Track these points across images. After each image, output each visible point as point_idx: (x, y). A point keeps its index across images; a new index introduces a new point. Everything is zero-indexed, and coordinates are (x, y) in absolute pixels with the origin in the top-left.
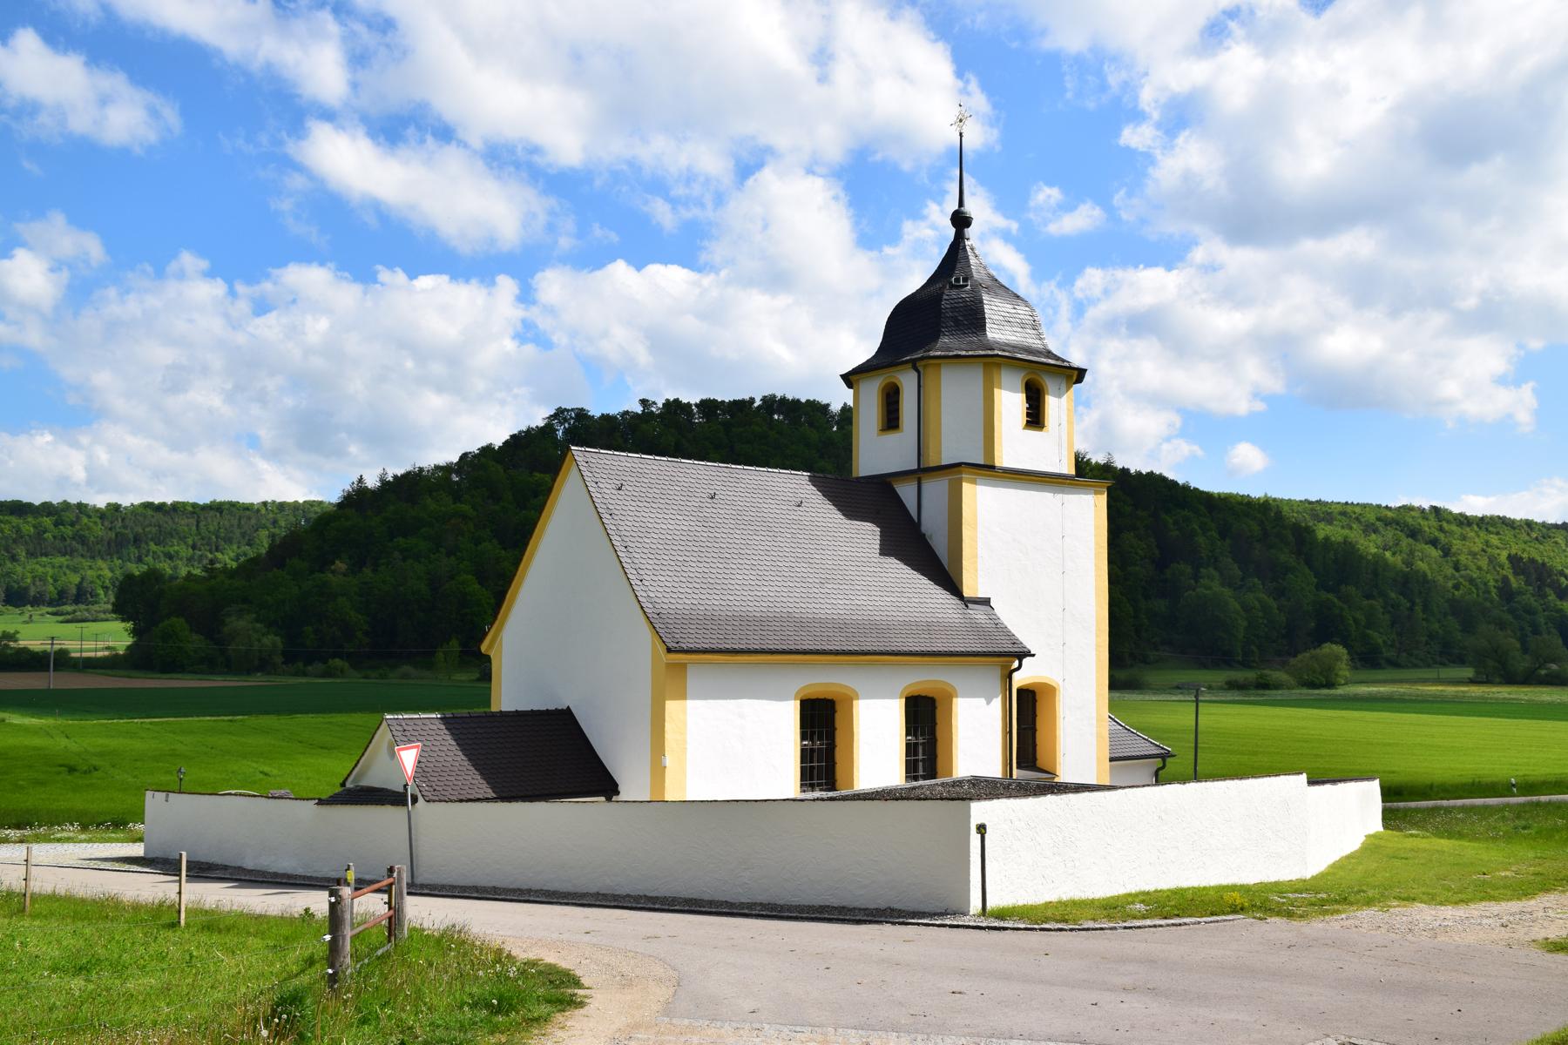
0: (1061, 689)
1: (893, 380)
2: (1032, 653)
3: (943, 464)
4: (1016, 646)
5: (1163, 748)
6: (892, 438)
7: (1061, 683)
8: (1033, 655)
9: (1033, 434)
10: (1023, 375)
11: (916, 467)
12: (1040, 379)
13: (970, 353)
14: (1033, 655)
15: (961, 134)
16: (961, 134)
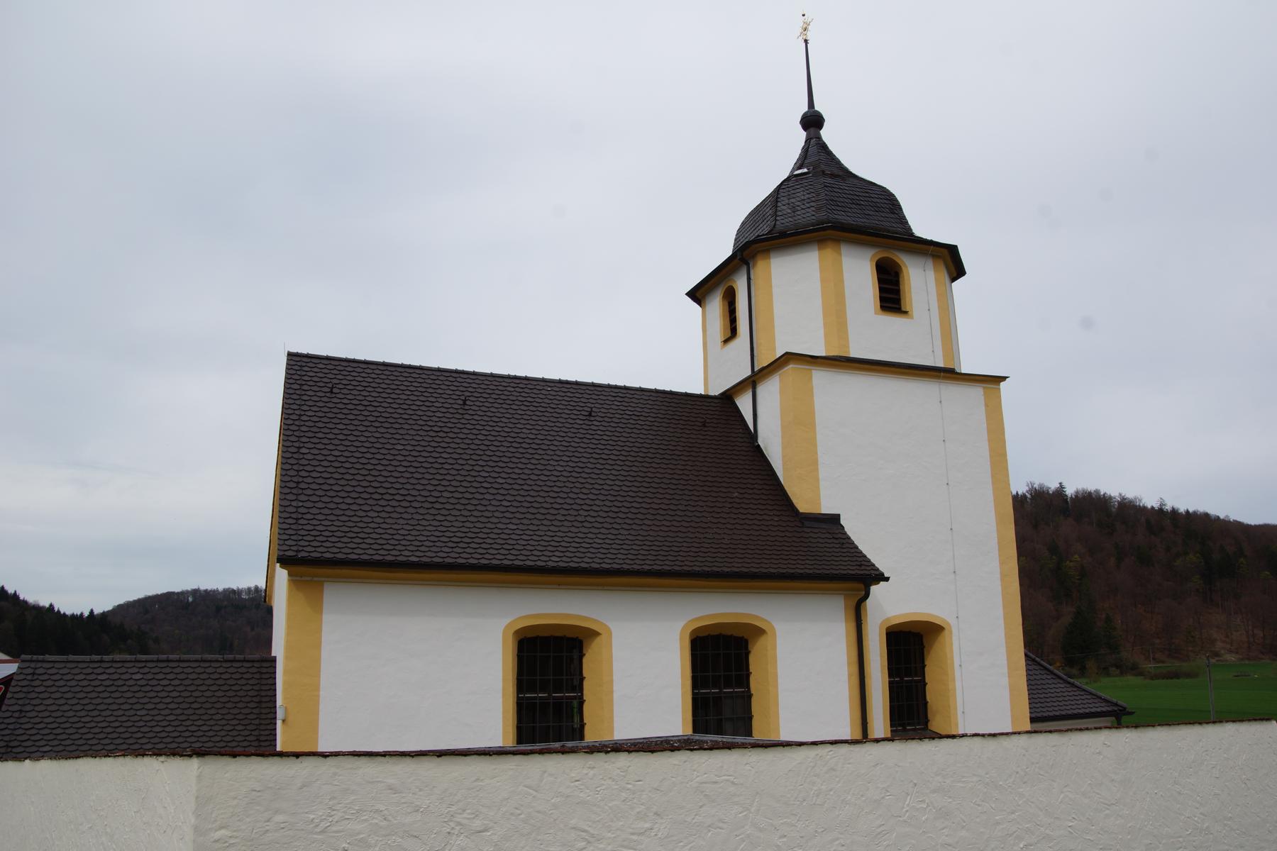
0: (954, 631)
2: (886, 575)
4: (863, 567)
5: (1116, 705)
6: (734, 344)
8: (887, 579)
12: (897, 260)
14: (887, 579)
15: (806, 41)
16: (806, 41)
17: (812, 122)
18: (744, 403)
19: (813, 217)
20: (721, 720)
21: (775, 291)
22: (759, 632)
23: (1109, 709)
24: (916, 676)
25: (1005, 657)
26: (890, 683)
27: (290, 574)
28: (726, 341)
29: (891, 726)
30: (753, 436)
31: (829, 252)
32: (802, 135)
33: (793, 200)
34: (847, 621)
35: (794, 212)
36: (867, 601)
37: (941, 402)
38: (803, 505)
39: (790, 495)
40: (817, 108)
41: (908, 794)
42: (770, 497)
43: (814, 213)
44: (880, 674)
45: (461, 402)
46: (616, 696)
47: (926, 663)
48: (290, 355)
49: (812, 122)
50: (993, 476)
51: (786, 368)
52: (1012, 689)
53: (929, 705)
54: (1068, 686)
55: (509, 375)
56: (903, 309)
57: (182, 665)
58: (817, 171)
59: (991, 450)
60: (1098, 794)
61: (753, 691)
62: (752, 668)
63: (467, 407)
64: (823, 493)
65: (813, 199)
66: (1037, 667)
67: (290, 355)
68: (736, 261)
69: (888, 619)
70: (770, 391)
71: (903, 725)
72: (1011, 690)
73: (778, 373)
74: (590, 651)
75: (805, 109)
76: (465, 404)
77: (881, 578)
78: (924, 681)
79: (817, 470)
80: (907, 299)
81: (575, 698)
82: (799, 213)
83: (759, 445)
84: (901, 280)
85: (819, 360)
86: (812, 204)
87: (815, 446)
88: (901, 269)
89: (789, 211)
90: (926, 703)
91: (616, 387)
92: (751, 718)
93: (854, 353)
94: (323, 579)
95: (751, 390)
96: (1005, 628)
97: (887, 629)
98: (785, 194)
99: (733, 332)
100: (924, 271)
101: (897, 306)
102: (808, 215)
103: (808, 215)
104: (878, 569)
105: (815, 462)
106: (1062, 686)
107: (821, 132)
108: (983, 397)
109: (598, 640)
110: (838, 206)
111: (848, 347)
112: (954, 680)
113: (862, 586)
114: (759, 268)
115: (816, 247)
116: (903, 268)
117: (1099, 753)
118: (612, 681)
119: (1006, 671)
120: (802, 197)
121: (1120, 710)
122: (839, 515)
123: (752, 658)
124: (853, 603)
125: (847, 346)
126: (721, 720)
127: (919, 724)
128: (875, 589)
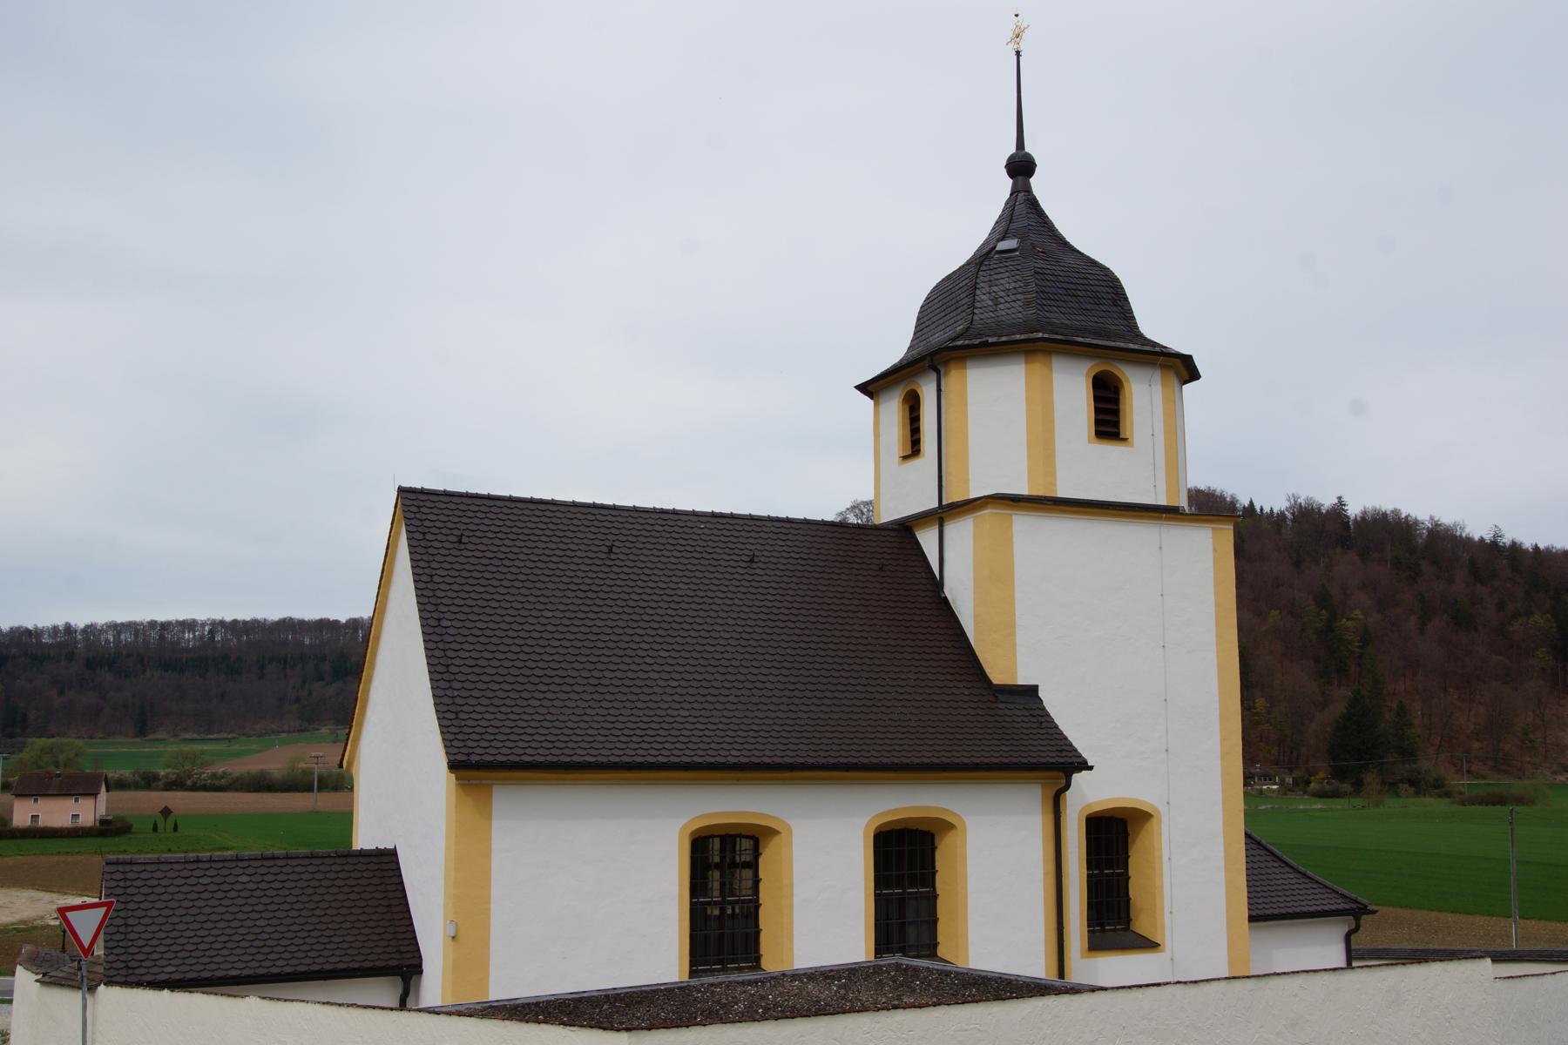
0: (1164, 819)
1: (915, 388)
3: (972, 496)
4: (1064, 754)
5: (1355, 901)
6: (915, 463)
7: (1161, 807)
8: (1091, 768)
9: (1109, 449)
10: (1085, 372)
11: (936, 505)
12: (1116, 373)
13: (1004, 339)
14: (1091, 768)
15: (1018, 53)
17: (1021, 167)
18: (927, 539)
19: (1020, 315)
20: (904, 924)
21: (971, 410)
22: (948, 826)
23: (1346, 906)
25: (1222, 848)
26: (1089, 876)
27: (456, 779)
28: (905, 458)
29: (1089, 926)
30: (938, 585)
31: (1038, 367)
32: (1007, 183)
33: (995, 289)
35: (996, 305)
37: (1160, 548)
38: (997, 677)
40: (1028, 149)
41: (1117, 1036)
42: (961, 664)
43: (1020, 309)
45: (606, 550)
46: (796, 900)
48: (401, 490)
49: (1021, 167)
51: (979, 514)
52: (1229, 885)
53: (1131, 902)
55: (654, 508)
56: (1121, 436)
57: (294, 862)
58: (1027, 250)
60: (1293, 1034)
61: (939, 891)
63: (613, 556)
64: (1020, 659)
65: (1020, 290)
66: (1262, 852)
67: (401, 490)
68: (926, 363)
69: (1089, 805)
70: (961, 533)
71: (1102, 925)
72: (1227, 887)
74: (767, 850)
75: (1013, 150)
76: (610, 552)
77: (1084, 766)
78: (1127, 874)
79: (1013, 634)
80: (1128, 423)
81: (750, 901)
82: (1001, 306)
83: (946, 597)
84: (1121, 397)
86: (1019, 296)
88: (1122, 384)
89: (990, 303)
90: (1128, 900)
91: (778, 520)
92: (935, 921)
93: (1062, 493)
94: (490, 782)
95: (937, 526)
98: (986, 279)
99: (914, 448)
100: (1150, 386)
101: (1114, 430)
102: (1013, 310)
103: (1013, 310)
105: (1013, 625)
107: (1032, 180)
108: (1211, 540)
109: (776, 840)
110: (1050, 299)
111: (1055, 485)
112: (1162, 875)
113: (1062, 774)
114: (952, 379)
115: (1023, 359)
116: (1125, 384)
117: (1295, 996)
118: (791, 885)
119: (1222, 864)
120: (1007, 286)
121: (1359, 909)
125: (1054, 484)
126: (904, 924)
127: (1119, 924)
128: (1078, 778)
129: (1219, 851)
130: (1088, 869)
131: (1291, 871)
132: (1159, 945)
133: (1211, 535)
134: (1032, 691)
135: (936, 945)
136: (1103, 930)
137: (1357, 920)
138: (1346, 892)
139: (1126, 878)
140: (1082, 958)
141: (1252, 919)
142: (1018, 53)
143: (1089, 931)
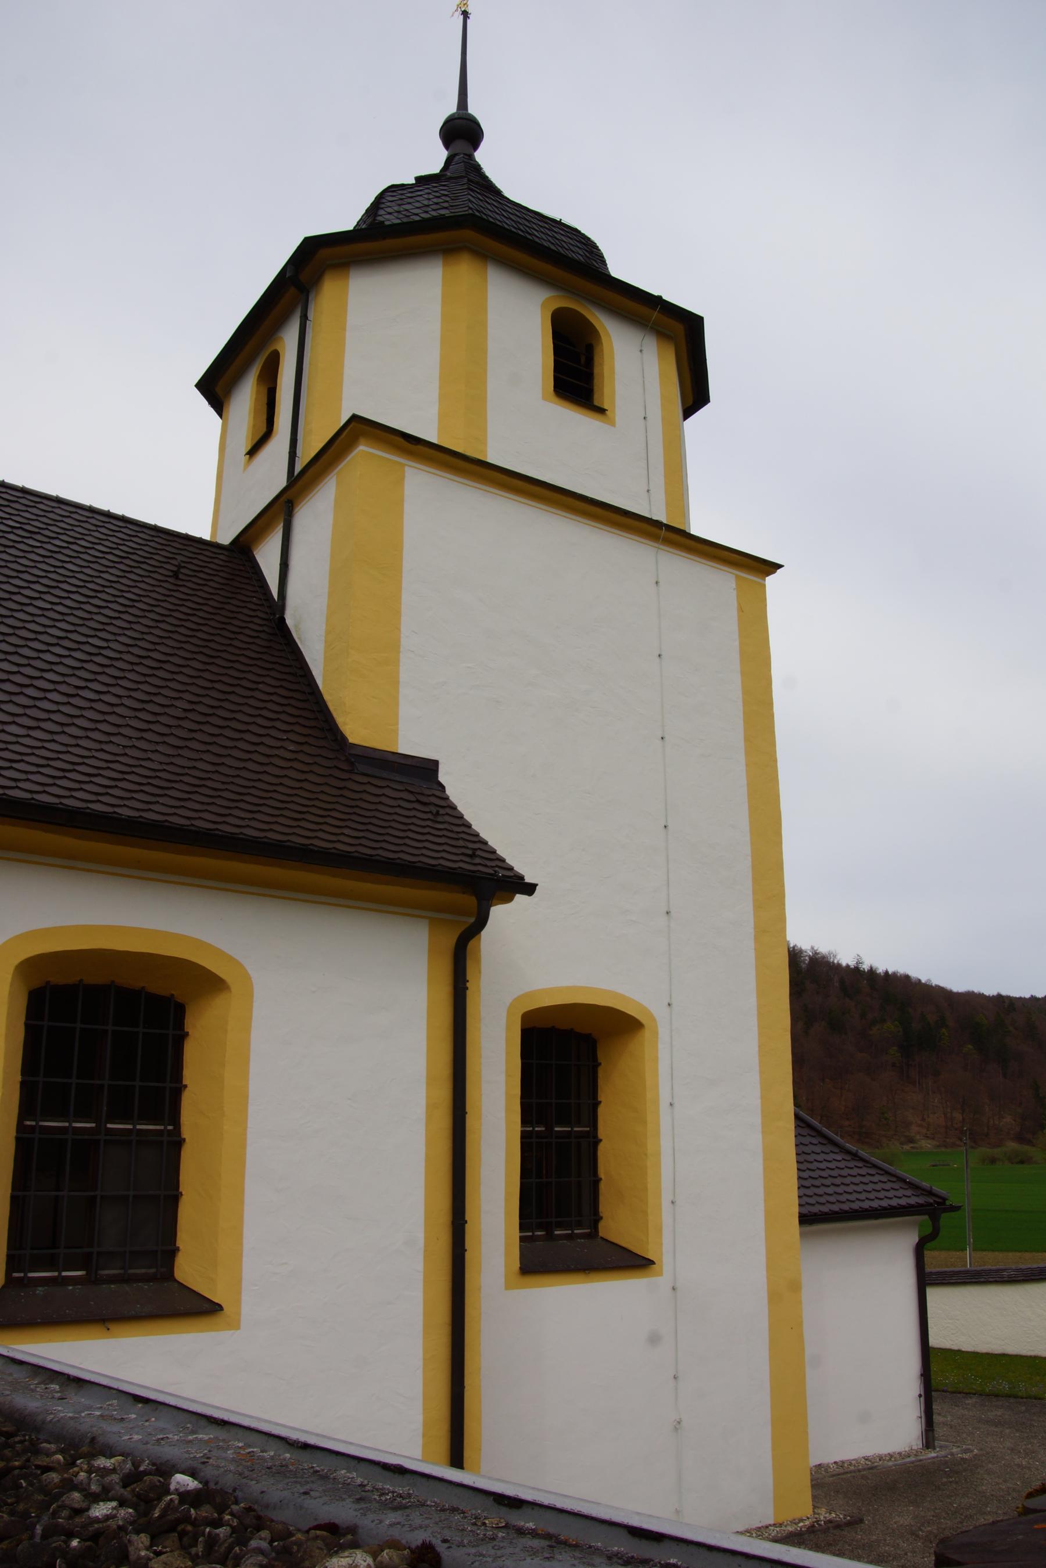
0: (663, 1032)
2: (528, 879)
4: (477, 861)
5: (930, 1193)
8: (530, 889)
14: (530, 889)
21: (351, 338)
23: (913, 1201)
24: (579, 1124)
25: (757, 1093)
26: (525, 1136)
29: (522, 1228)
34: (430, 981)
36: (483, 933)
39: (331, 708)
44: (502, 1114)
47: (601, 1097)
50: (747, 739)
51: (349, 458)
52: (769, 1155)
54: (848, 1157)
59: (746, 692)
61: (186, 1132)
62: (189, 1075)
64: (405, 710)
65: (446, 205)
71: (548, 1228)
72: (765, 1159)
73: (336, 471)
78: (595, 1136)
79: (397, 662)
85: (420, 447)
87: (398, 613)
90: (596, 1182)
96: (760, 1034)
97: (527, 1017)
104: (511, 869)
105: (395, 646)
106: (839, 1157)
108: (735, 592)
119: (758, 1120)
120: (426, 202)
121: (938, 1203)
122: (436, 763)
123: (191, 1051)
124: (449, 940)
125: (483, 441)
127: (579, 1225)
129: (753, 1098)
130: (524, 1122)
131: (836, 1150)
132: (653, 1262)
133: (734, 586)
134: (428, 769)
135: (172, 1252)
136: (550, 1237)
137: (935, 1219)
138: (916, 1180)
139: (593, 1141)
140: (508, 1286)
141: (805, 1219)
142: (465, 14)
143: (522, 1239)
